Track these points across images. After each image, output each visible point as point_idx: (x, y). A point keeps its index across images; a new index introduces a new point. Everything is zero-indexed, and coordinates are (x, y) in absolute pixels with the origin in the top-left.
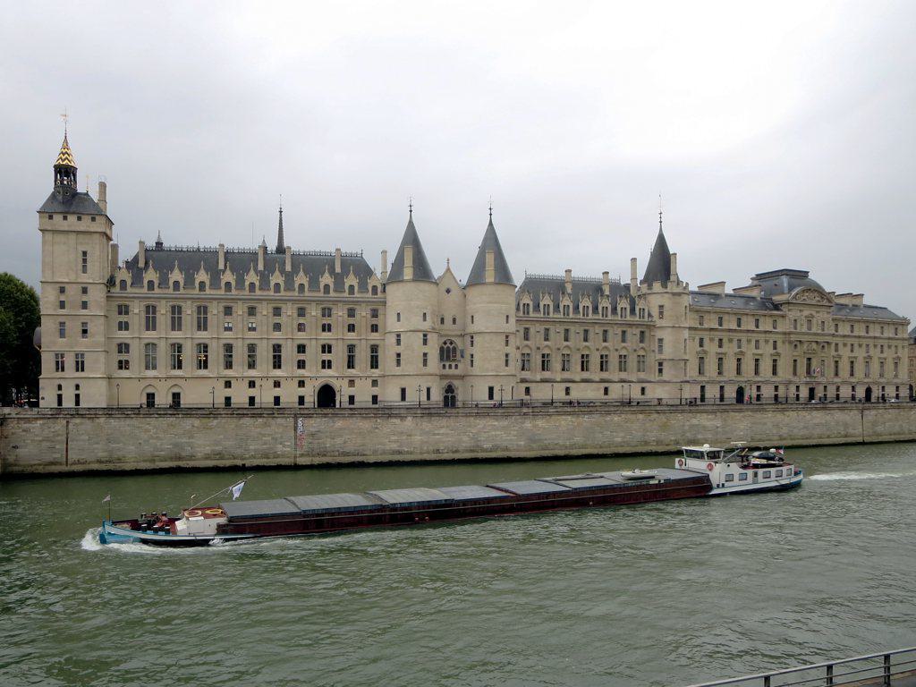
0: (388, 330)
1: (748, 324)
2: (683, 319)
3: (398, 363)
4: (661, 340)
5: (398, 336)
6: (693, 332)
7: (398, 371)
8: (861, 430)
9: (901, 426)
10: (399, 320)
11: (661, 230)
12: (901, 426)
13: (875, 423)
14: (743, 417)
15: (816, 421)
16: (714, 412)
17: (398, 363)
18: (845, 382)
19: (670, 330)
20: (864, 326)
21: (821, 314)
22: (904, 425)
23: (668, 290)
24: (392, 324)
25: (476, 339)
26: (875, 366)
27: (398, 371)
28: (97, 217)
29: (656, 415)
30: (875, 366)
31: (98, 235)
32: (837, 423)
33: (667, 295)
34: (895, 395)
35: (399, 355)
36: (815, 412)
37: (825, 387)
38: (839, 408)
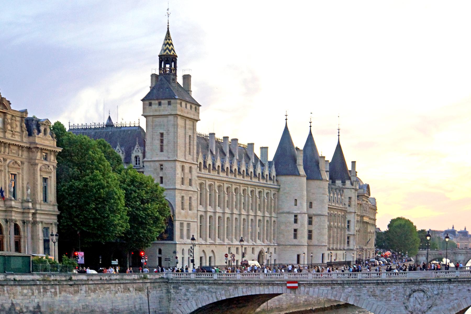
0: (281, 211)
3: (295, 236)
4: (349, 222)
5: (296, 216)
7: (295, 242)
10: (296, 205)
11: (310, 131)
17: (295, 236)
19: (353, 214)
23: (354, 187)
24: (288, 205)
25: (315, 219)
27: (295, 242)
28: (197, 107)
31: (173, 116)
33: (353, 191)
35: (295, 230)
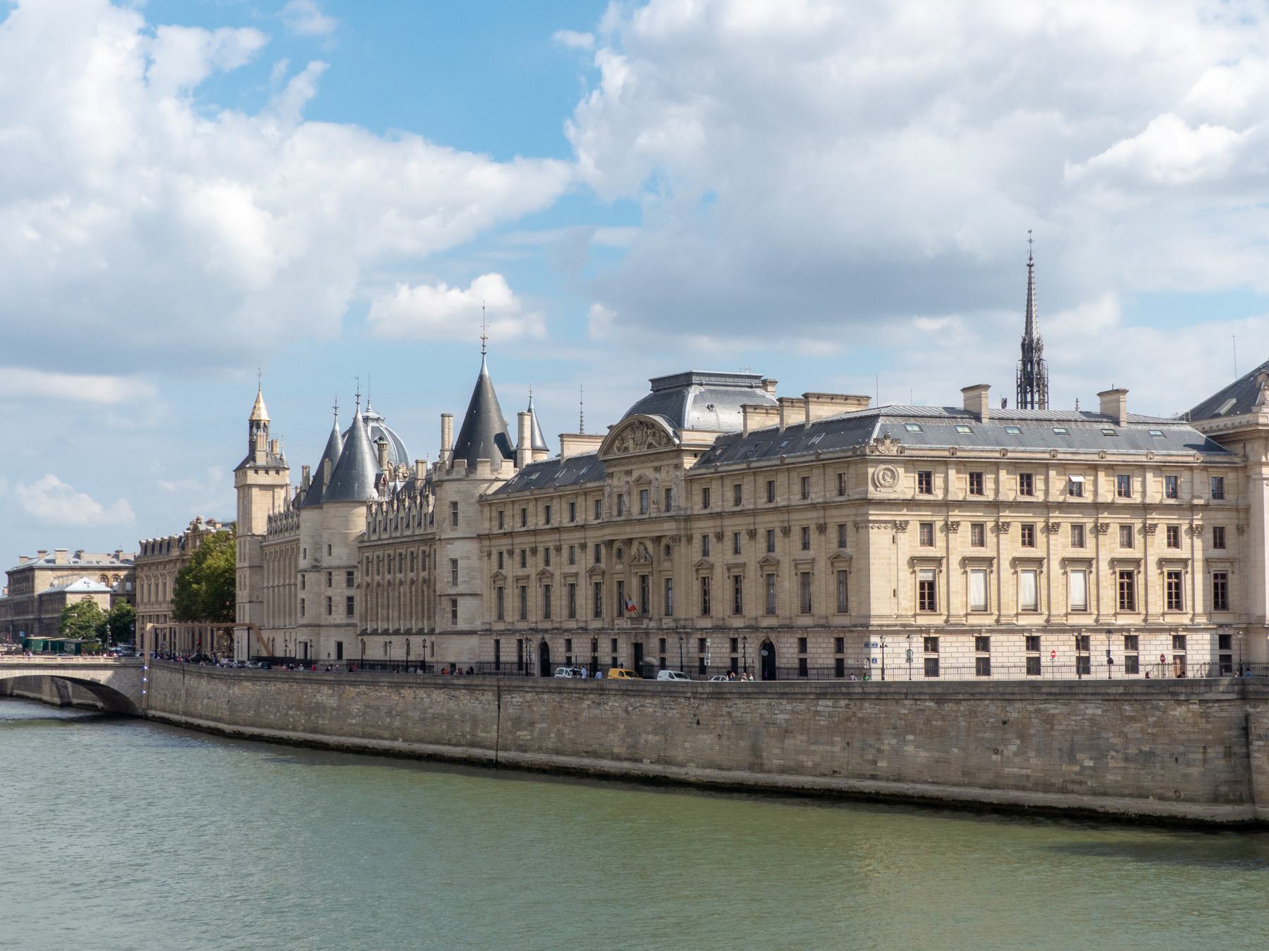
1: (561, 517)
2: (447, 524)
6: (486, 543)
8: (494, 735)
9: (560, 735)
12: (560, 735)
13: (517, 722)
14: (358, 694)
15: (437, 709)
16: (331, 684)
18: (720, 629)
20: (796, 478)
21: (663, 475)
22: (567, 731)
26: (788, 585)
29: (295, 686)
30: (788, 585)
32: (463, 715)
34: (796, 663)
36: (437, 692)
37: (663, 641)
38: (465, 686)
